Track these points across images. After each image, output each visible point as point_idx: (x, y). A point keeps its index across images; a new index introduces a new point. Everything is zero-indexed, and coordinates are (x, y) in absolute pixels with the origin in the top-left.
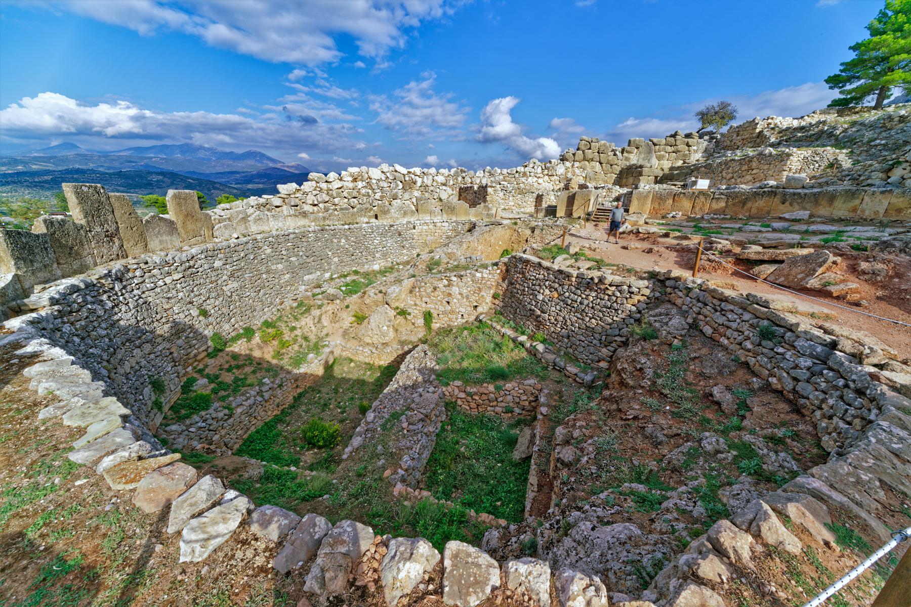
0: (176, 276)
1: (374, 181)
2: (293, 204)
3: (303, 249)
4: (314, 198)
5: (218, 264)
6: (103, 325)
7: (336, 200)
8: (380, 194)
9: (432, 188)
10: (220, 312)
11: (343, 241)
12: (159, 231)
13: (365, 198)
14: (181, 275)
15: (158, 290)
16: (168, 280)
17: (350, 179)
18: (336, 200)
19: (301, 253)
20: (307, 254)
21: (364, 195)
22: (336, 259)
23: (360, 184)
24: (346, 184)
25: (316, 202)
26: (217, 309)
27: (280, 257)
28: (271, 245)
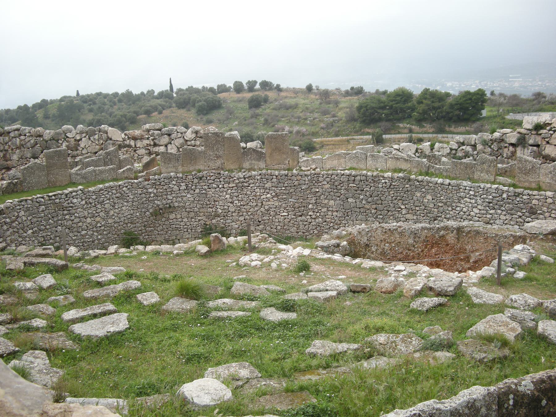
0: (230, 186)
2: (531, 142)
3: (368, 194)
5: (268, 185)
6: (173, 195)
10: (252, 217)
11: (429, 197)
12: (251, 157)
14: (234, 185)
15: (217, 189)
19: (362, 197)
20: (370, 199)
22: (408, 216)
26: (249, 213)
27: (339, 194)
28: (332, 182)
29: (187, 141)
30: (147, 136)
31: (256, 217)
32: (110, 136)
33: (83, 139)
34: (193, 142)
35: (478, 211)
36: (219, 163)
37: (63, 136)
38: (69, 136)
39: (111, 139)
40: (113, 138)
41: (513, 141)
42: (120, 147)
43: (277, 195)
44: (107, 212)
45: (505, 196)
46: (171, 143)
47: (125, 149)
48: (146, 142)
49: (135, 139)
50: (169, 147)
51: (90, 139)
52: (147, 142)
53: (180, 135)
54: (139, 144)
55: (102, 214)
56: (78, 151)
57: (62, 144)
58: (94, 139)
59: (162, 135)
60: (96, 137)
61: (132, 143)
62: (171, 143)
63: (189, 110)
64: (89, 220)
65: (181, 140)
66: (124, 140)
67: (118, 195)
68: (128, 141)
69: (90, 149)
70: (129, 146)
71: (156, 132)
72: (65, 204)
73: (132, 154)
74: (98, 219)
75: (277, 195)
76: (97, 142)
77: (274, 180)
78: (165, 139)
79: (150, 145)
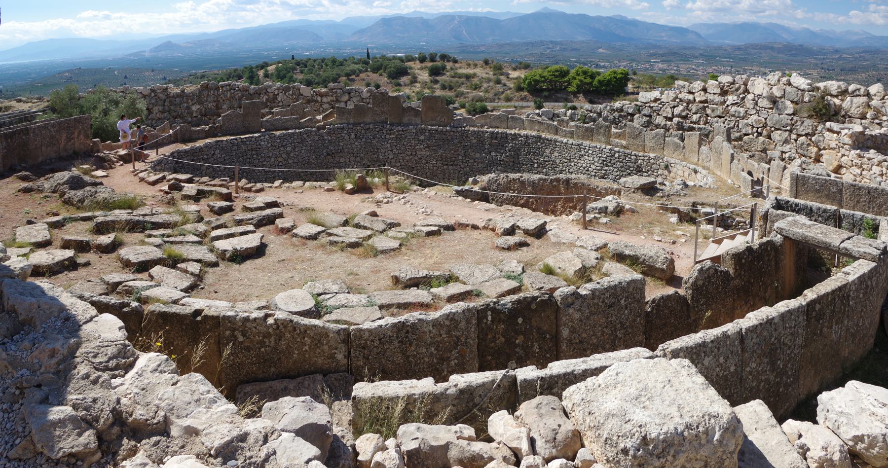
4: (669, 109)
5: (422, 138)
8: (755, 117)
13: (733, 118)
16: (388, 137)
18: (695, 118)
21: (733, 116)
25: (670, 115)
31: (410, 164)
36: (383, 118)
41: (630, 111)
42: (309, 102)
43: (428, 147)
44: (288, 154)
48: (330, 98)
49: (321, 95)
50: (349, 103)
52: (331, 98)
54: (325, 100)
55: (284, 156)
59: (344, 93)
61: (319, 99)
63: (381, 75)
64: (273, 160)
65: (358, 98)
66: (313, 96)
67: (299, 140)
69: (285, 102)
70: (317, 101)
71: (339, 91)
72: (255, 146)
74: (280, 159)
75: (428, 147)
77: (427, 134)
78: (346, 97)
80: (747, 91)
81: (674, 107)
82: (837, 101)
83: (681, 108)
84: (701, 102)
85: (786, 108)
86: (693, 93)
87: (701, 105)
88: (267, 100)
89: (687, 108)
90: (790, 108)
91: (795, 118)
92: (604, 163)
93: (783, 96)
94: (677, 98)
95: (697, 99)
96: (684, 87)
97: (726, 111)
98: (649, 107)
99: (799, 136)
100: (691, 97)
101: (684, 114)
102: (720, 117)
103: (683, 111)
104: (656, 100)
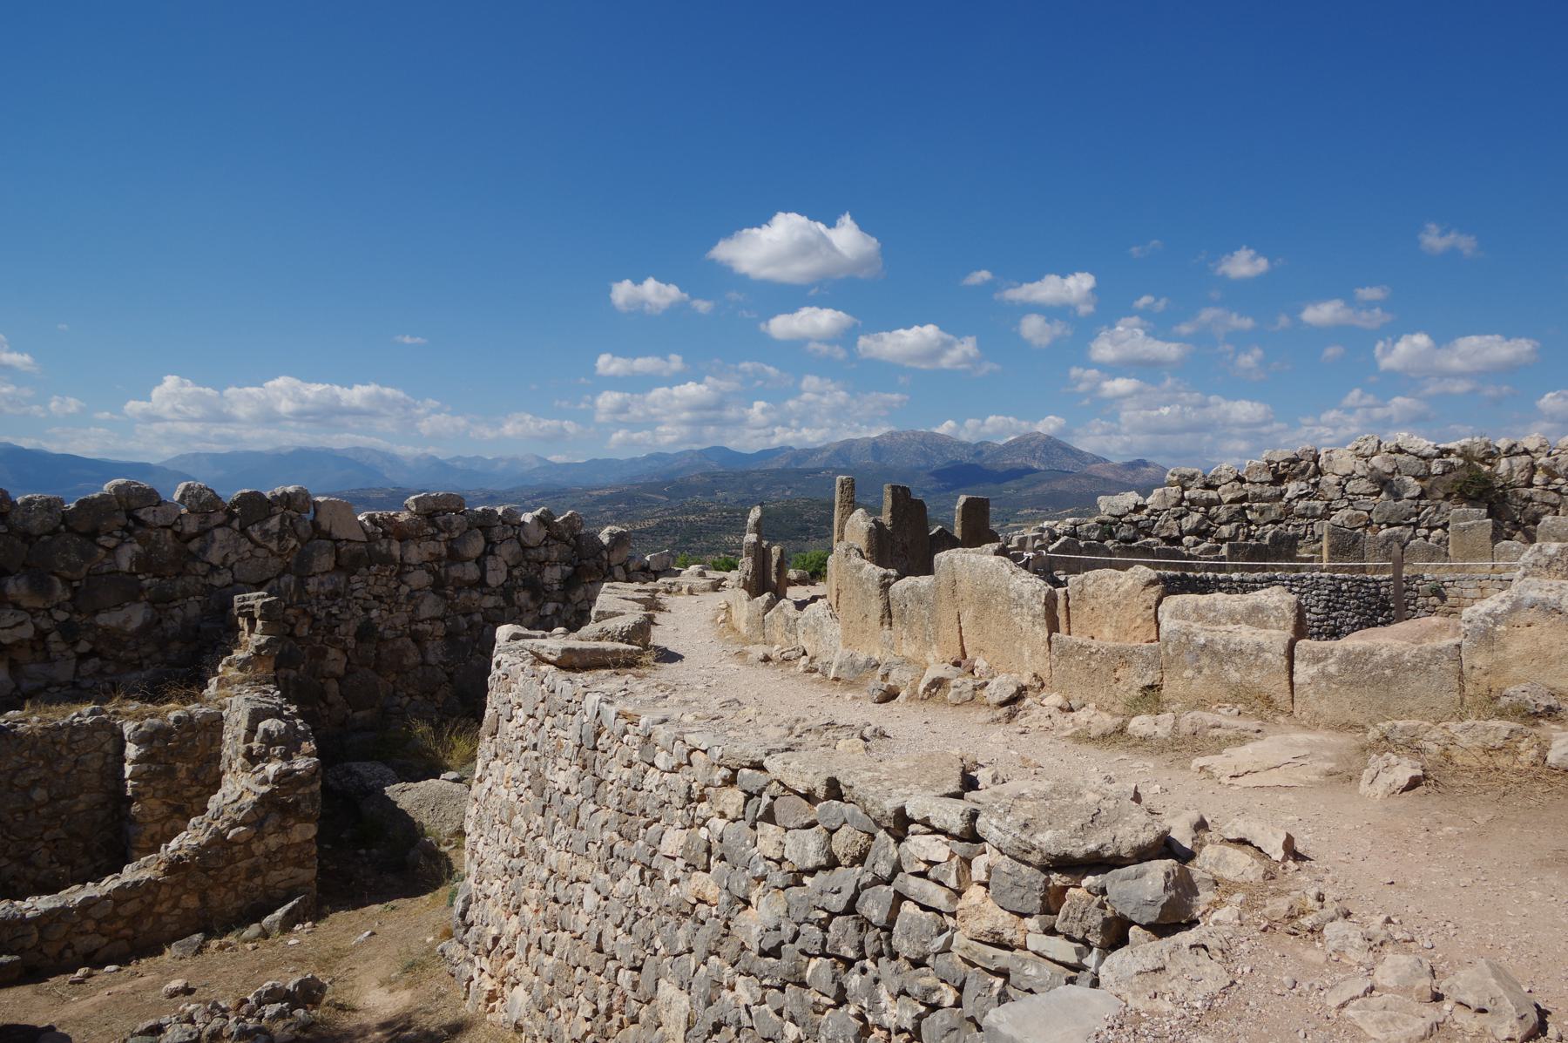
1: (1332, 479)
4: (1172, 523)
7: (1225, 531)
8: (1349, 512)
9: (1526, 492)
13: (1301, 521)
17: (1269, 477)
18: (1225, 531)
23: (1292, 488)
24: (1257, 489)
25: (1176, 534)
29: (525, 548)
30: (430, 530)
32: (325, 524)
33: (219, 534)
34: (542, 550)
35: (1314, 617)
37: (122, 519)
38: (150, 518)
39: (328, 536)
40: (336, 534)
45: (1344, 587)
46: (492, 553)
47: (374, 569)
50: (490, 563)
51: (243, 530)
52: (432, 547)
53: (510, 533)
54: (414, 554)
56: (190, 579)
57: (111, 551)
58: (265, 533)
60: (274, 523)
61: (396, 548)
62: (492, 553)
68: (384, 543)
70: (386, 559)
73: (393, 585)
76: (274, 545)
78: (476, 546)
79: (438, 558)
80: (1319, 472)
81: (1180, 517)
82: (1486, 468)
83: (1196, 517)
84: (1232, 501)
85: (1406, 488)
86: (1215, 488)
87: (1237, 506)
88: (144, 563)
89: (1206, 516)
90: (1414, 487)
91: (1423, 502)
92: (1330, 607)
93: (1397, 470)
94: (1183, 499)
95: (1227, 497)
96: (1192, 478)
97: (1288, 511)
98: (1131, 522)
99: (1431, 529)
100: (1212, 494)
101: (1204, 527)
102: (1275, 522)
103: (1200, 522)
104: (1138, 508)
